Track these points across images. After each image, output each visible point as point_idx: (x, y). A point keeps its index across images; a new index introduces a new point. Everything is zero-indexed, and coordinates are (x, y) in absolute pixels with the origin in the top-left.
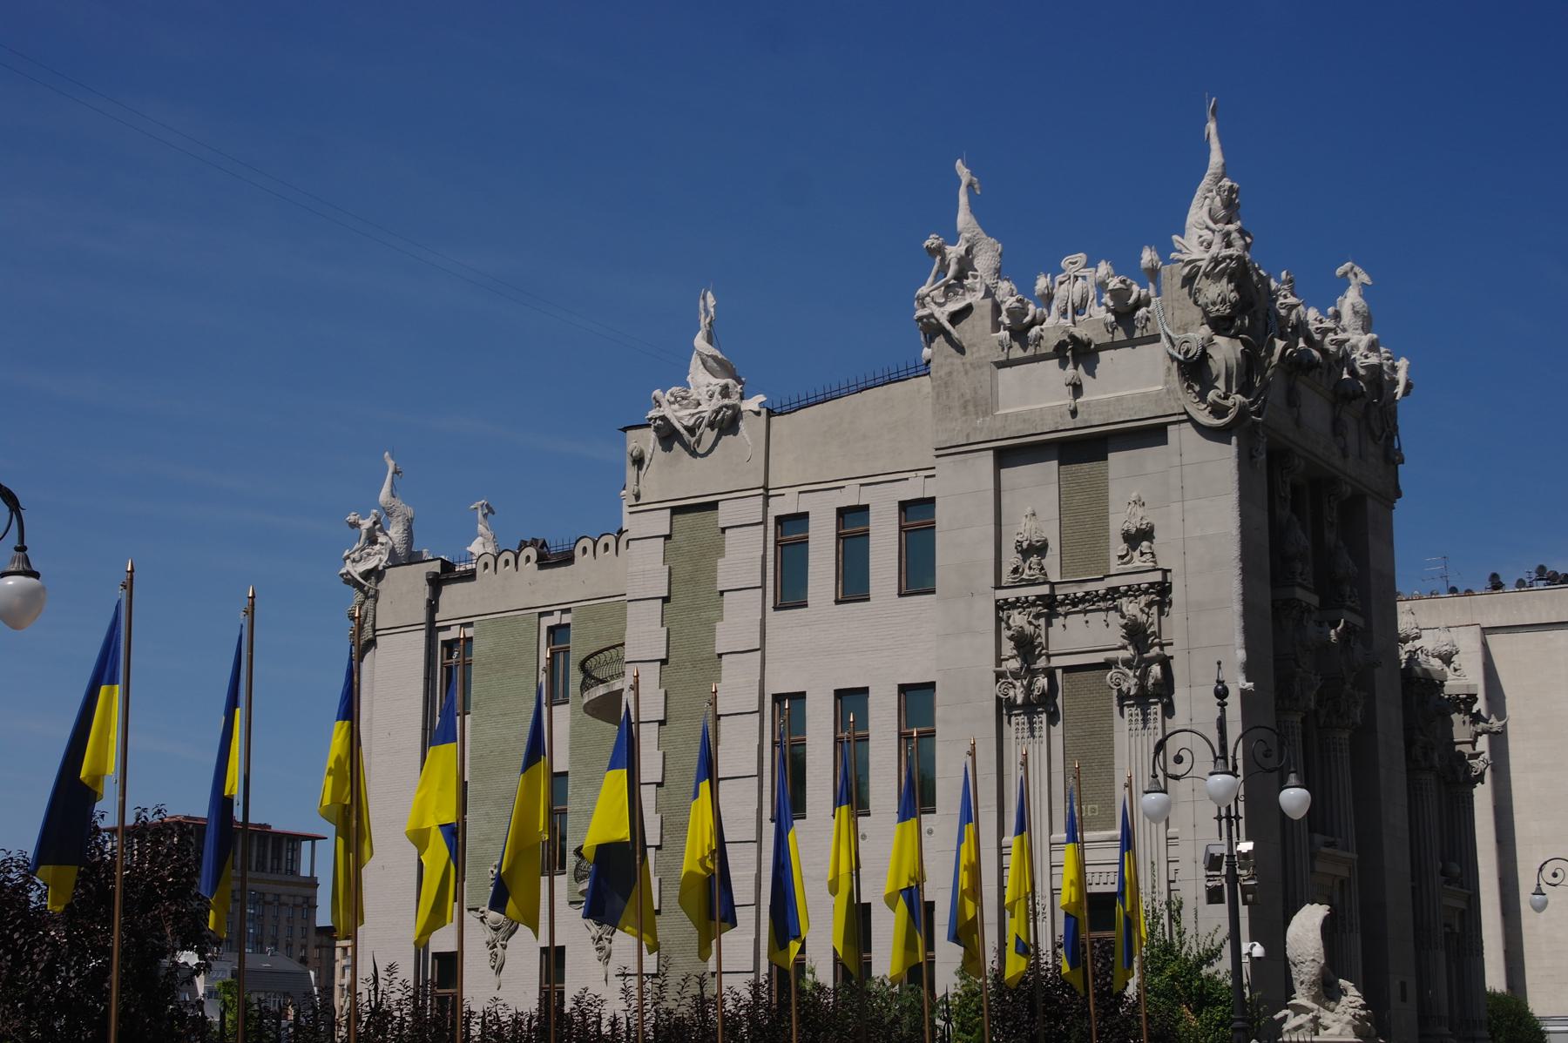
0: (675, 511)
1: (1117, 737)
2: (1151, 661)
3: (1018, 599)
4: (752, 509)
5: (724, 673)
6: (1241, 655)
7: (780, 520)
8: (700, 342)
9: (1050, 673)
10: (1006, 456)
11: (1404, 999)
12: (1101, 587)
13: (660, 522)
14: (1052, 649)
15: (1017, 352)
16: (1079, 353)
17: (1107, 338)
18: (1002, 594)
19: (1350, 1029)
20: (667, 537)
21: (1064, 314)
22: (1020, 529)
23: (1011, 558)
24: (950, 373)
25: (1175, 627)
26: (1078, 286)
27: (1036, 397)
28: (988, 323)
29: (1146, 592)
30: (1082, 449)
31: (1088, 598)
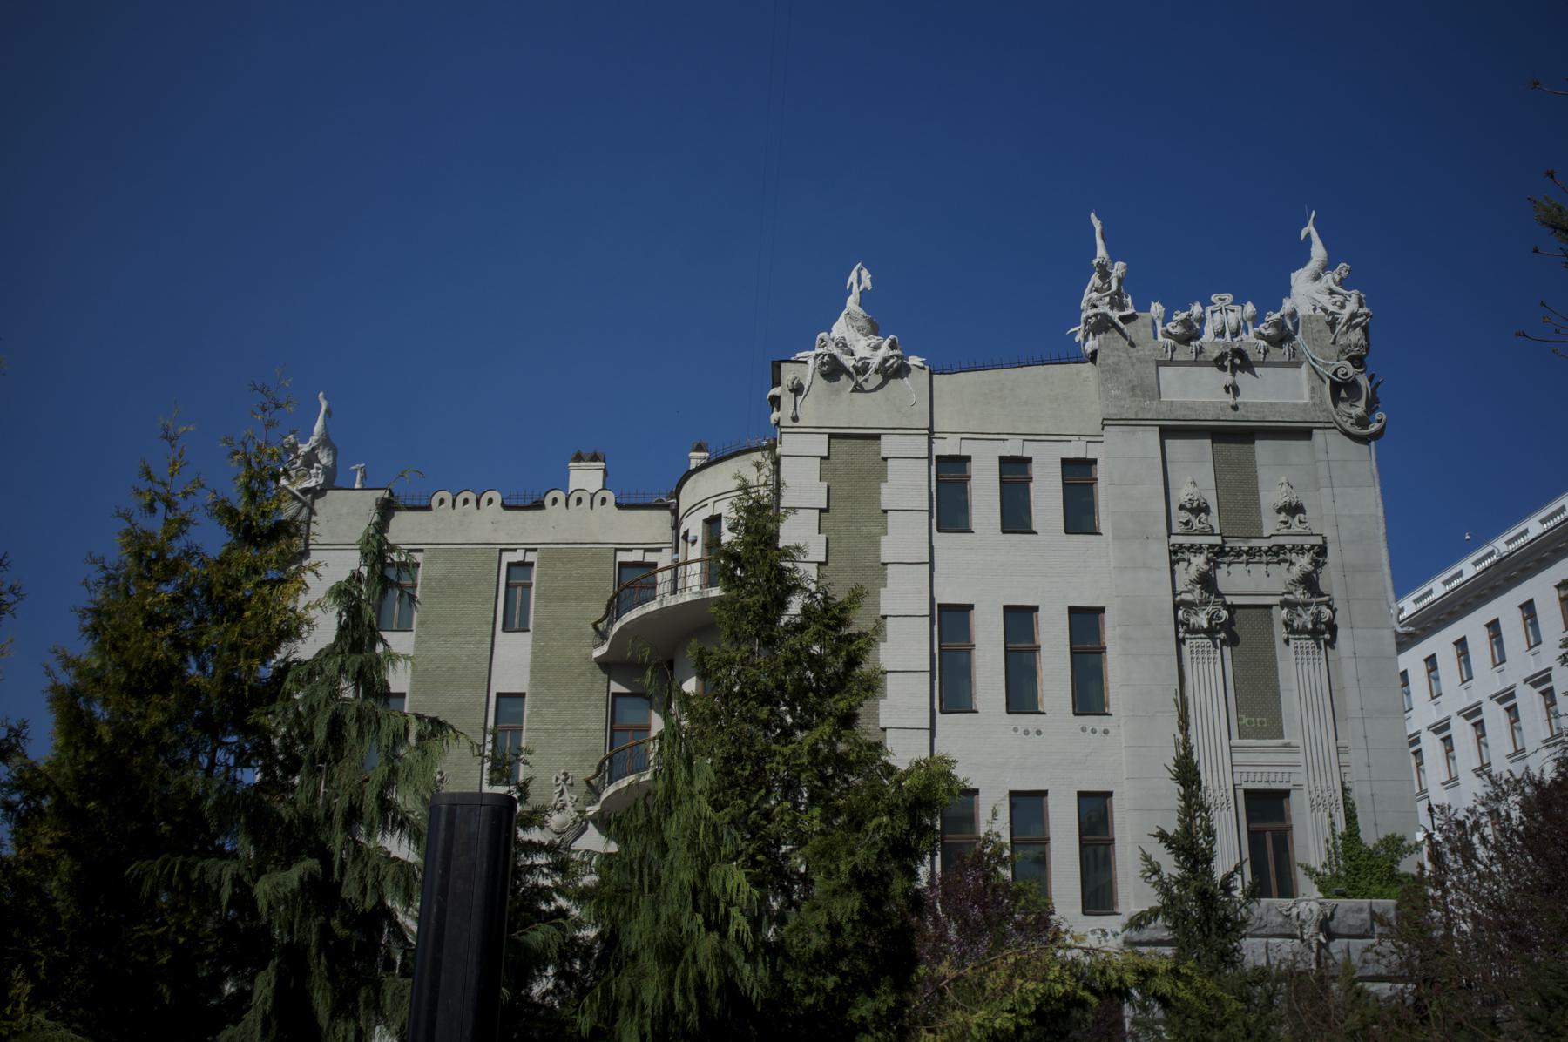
0: (831, 436)
1: (1281, 665)
3: (1192, 546)
4: (919, 445)
5: (889, 580)
8: (852, 303)
10: (1167, 432)
12: (1265, 545)
13: (820, 445)
18: (1175, 540)
22: (1182, 494)
23: (1179, 517)
24: (1117, 363)
26: (1222, 316)
27: (1197, 390)
30: (1233, 435)
31: (1252, 553)
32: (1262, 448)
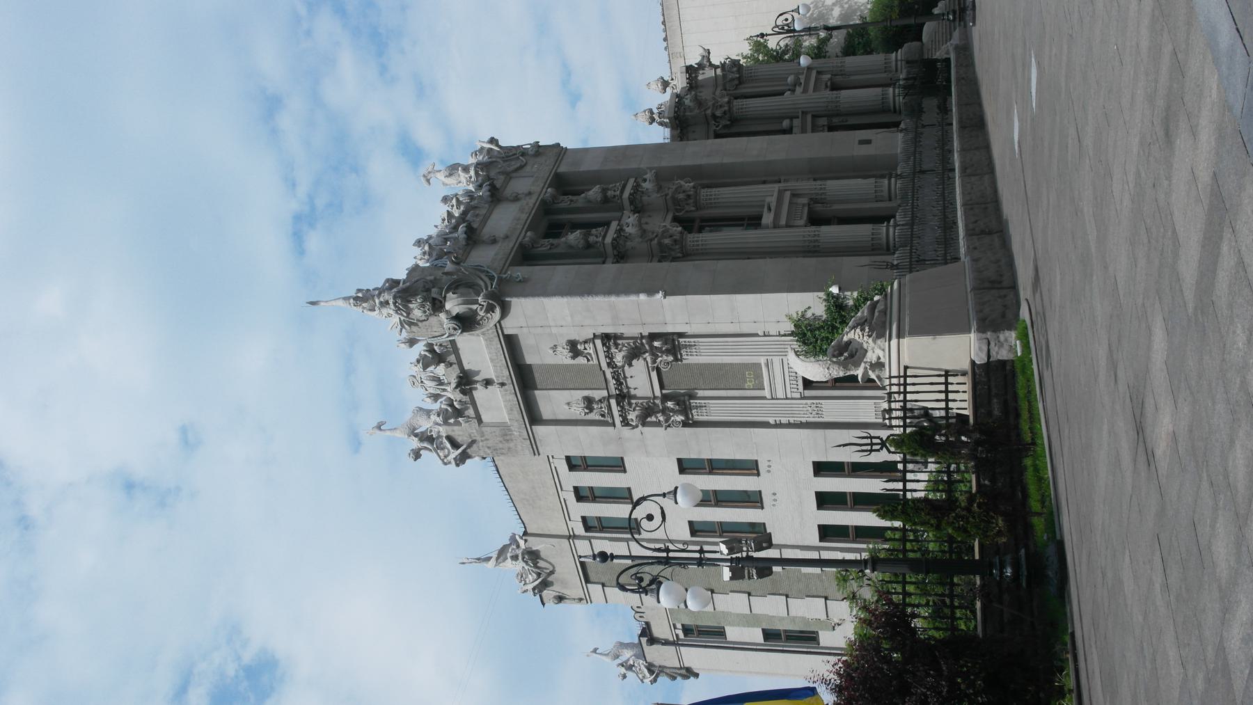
2: (652, 347)
6: (643, 297)
7: (587, 530)
9: (665, 398)
11: (868, 142)
14: (650, 395)
15: (471, 412)
16: (466, 381)
17: (455, 366)
19: (879, 342)
20: (603, 585)
21: (444, 390)
25: (631, 330)
28: (456, 428)
29: (609, 348)
30: (525, 379)
32: (530, 359)
